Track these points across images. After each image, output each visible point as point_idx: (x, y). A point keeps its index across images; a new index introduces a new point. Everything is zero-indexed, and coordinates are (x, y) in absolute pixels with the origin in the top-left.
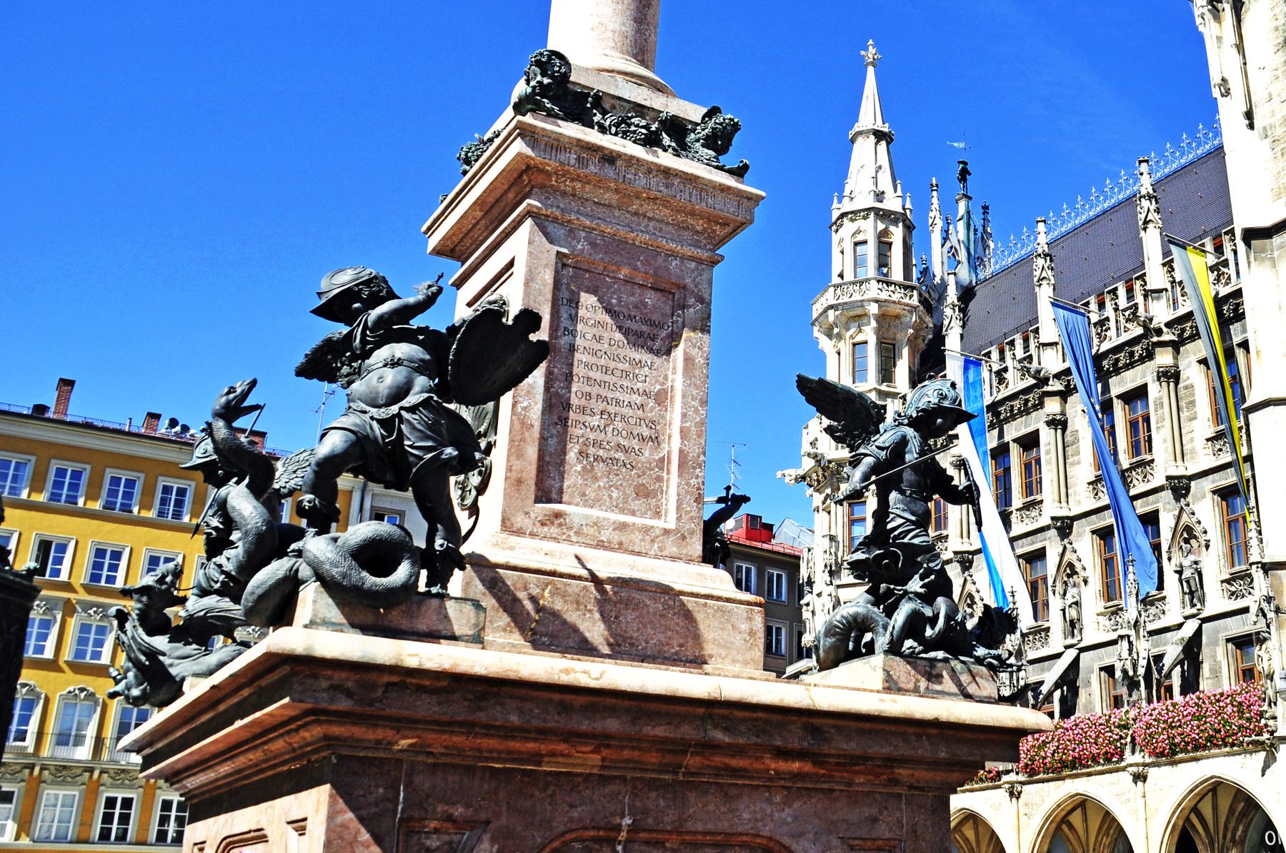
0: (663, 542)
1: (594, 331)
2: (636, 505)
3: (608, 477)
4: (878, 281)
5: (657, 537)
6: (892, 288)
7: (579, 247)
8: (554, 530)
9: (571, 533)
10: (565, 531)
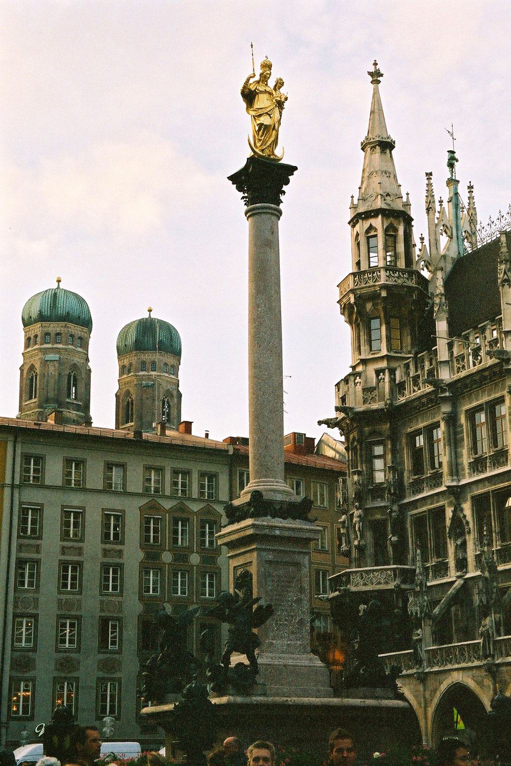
4: (386, 270)
6: (396, 275)
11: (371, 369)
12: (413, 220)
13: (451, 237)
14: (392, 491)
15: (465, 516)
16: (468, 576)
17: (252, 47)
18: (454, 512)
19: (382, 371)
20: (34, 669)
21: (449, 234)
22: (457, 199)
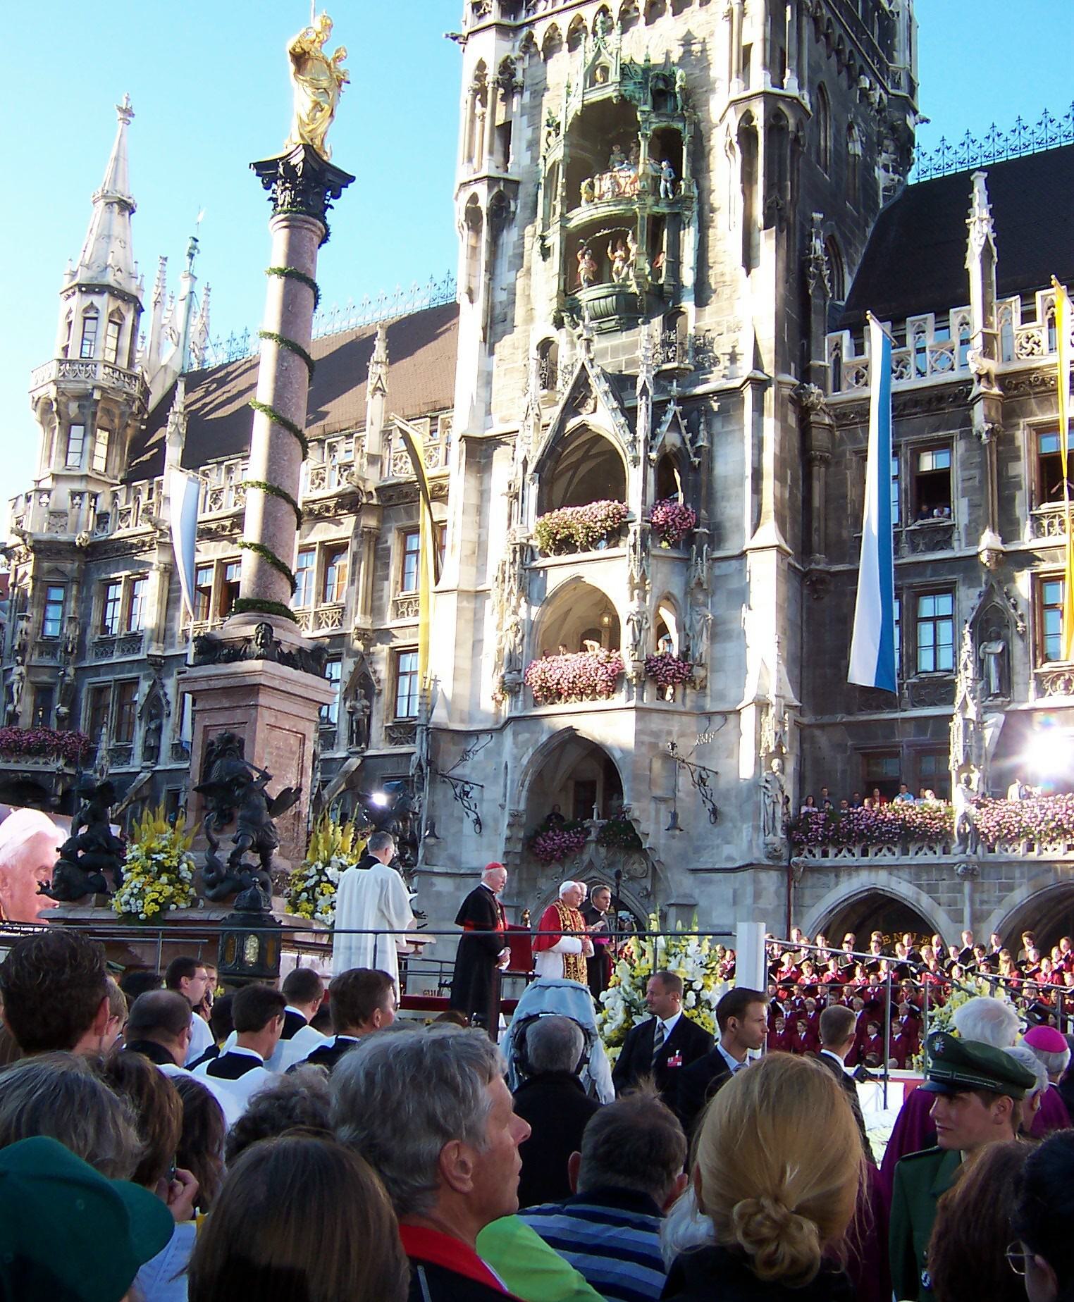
11: (65, 489)
12: (143, 310)
13: (177, 345)
14: (70, 649)
15: (165, 694)
16: (157, 768)
18: (152, 687)
19: (81, 494)
21: (175, 340)
22: (191, 300)
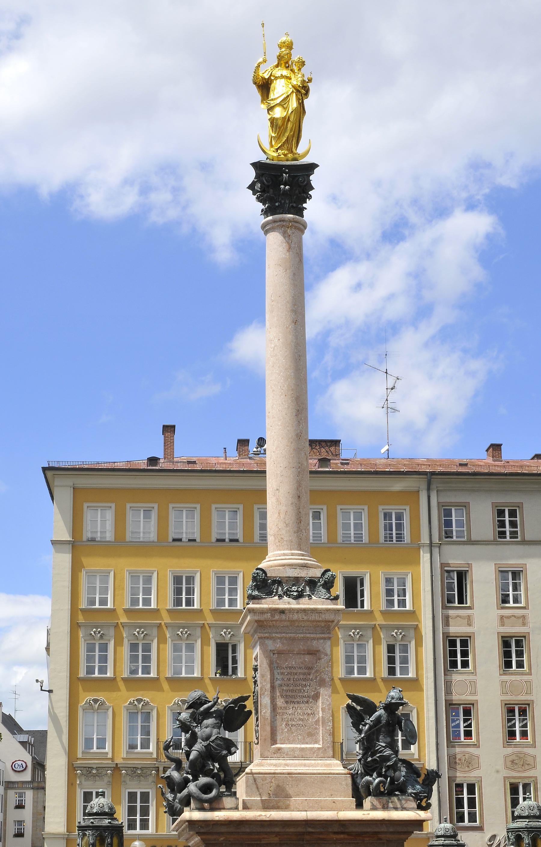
0: (318, 753)
1: (287, 677)
2: (308, 740)
3: (297, 732)
5: (315, 751)
7: (278, 646)
8: (278, 755)
9: (285, 755)
10: (282, 754)
17: (263, 26)
20: (478, 767)
